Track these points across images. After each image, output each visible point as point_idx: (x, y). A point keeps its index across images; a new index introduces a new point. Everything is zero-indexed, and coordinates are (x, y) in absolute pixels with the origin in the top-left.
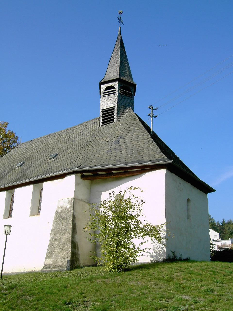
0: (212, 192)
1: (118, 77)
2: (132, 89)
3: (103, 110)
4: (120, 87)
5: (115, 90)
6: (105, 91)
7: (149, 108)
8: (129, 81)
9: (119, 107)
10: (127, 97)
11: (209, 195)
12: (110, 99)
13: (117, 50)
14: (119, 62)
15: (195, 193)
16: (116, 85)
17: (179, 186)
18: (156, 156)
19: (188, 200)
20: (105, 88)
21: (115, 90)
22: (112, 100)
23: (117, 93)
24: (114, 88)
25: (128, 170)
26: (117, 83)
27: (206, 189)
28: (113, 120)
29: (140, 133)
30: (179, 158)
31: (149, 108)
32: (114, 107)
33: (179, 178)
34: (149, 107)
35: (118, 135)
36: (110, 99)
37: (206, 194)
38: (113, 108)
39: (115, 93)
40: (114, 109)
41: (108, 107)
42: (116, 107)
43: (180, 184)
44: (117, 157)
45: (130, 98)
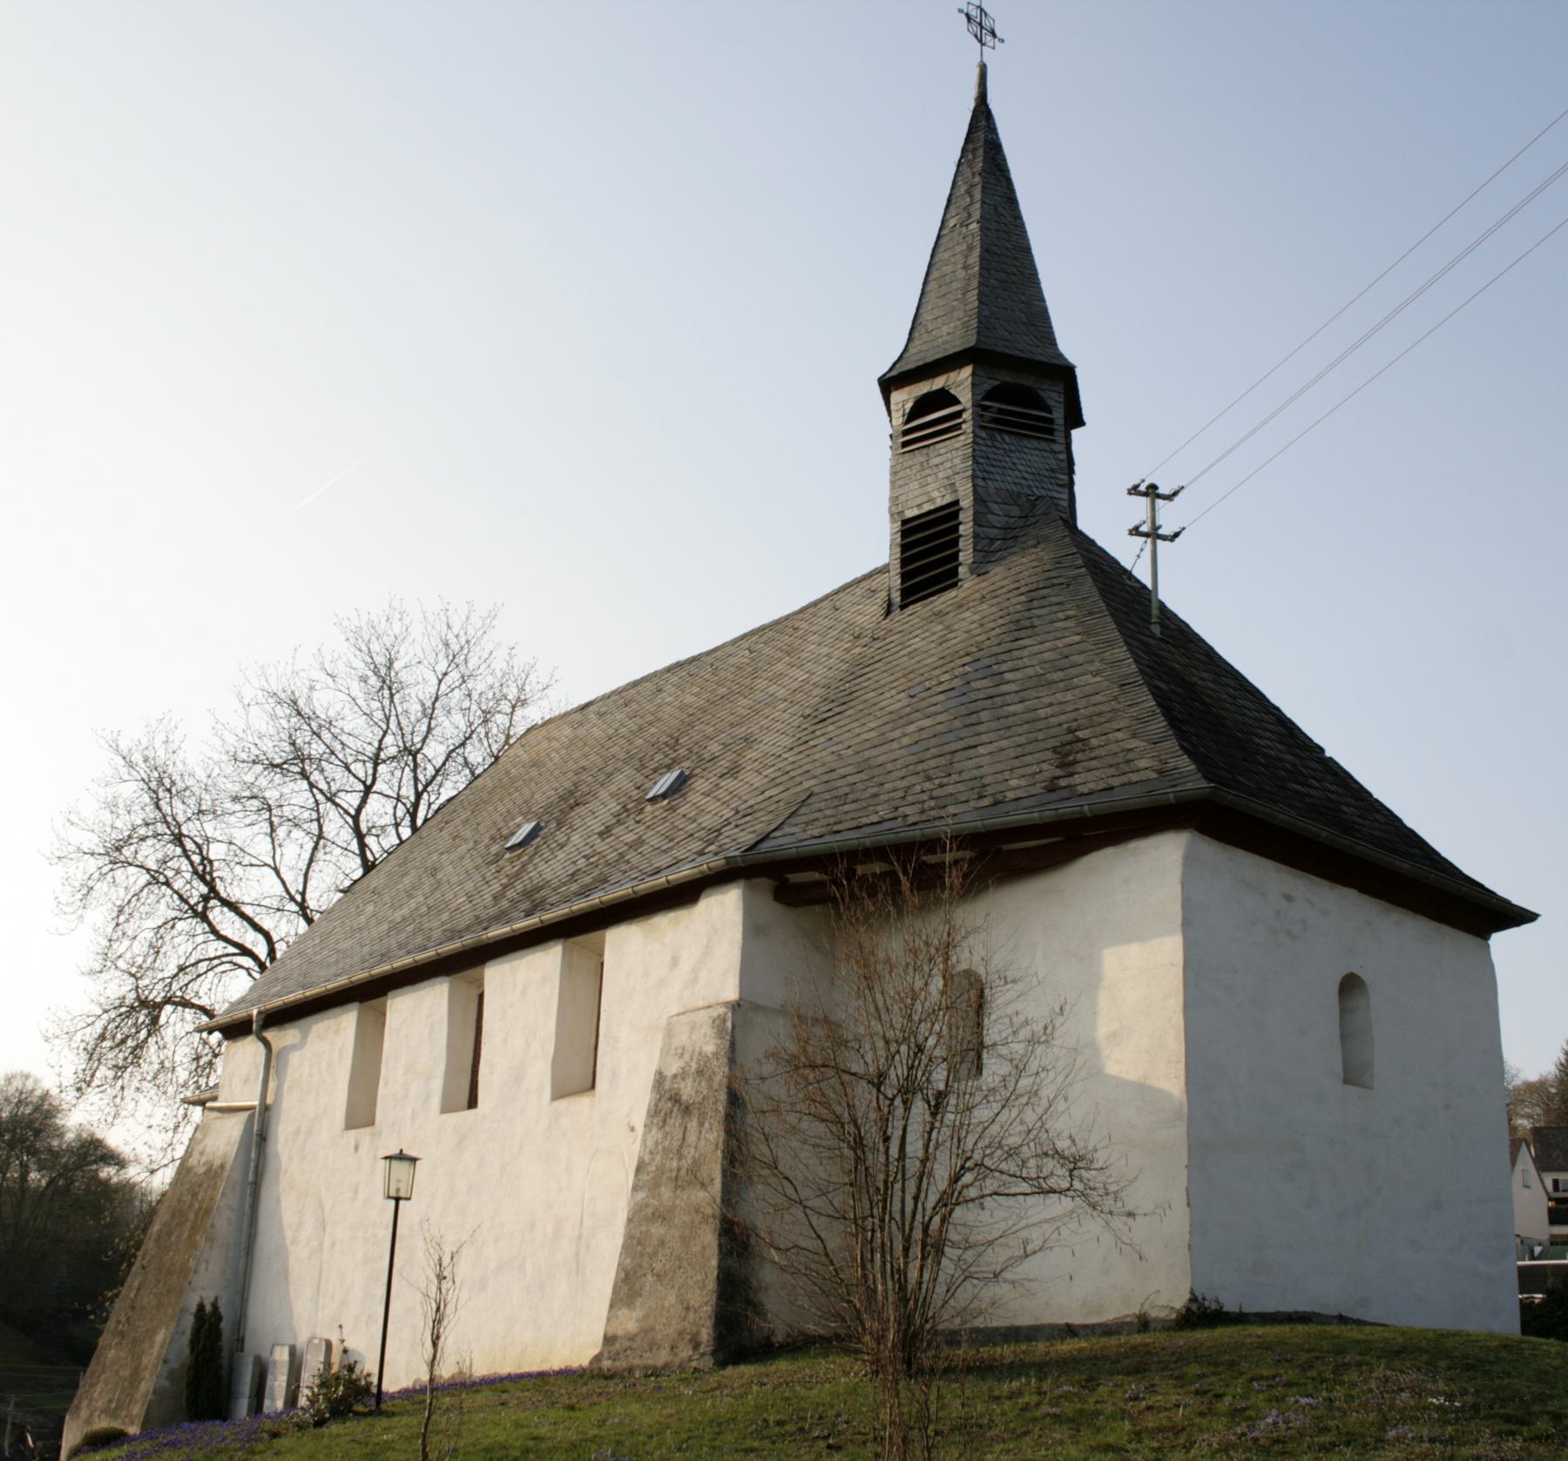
0: (1518, 925)
1: (971, 341)
2: (1054, 395)
3: (904, 522)
4: (986, 398)
5: (958, 414)
6: (907, 422)
7: (1134, 491)
8: (1040, 355)
9: (979, 500)
10: (1026, 442)
11: (1500, 942)
12: (937, 460)
13: (969, 193)
14: (974, 258)
15: (1389, 941)
16: (961, 382)
17: (1278, 913)
18: (1142, 763)
19: (1350, 986)
20: (909, 406)
21: (958, 414)
22: (948, 465)
23: (968, 427)
24: (956, 401)
25: (1005, 847)
26: (967, 372)
27: (1482, 913)
28: (954, 572)
29: (1077, 638)
30: (1322, 750)
31: (1134, 491)
32: (957, 502)
33: (1280, 866)
34: (1135, 488)
35: (967, 659)
36: (937, 460)
37: (1484, 934)
38: (950, 512)
39: (958, 427)
40: (955, 515)
41: (927, 508)
42: (966, 503)
43: (1288, 898)
44: (945, 781)
45: (1044, 445)
